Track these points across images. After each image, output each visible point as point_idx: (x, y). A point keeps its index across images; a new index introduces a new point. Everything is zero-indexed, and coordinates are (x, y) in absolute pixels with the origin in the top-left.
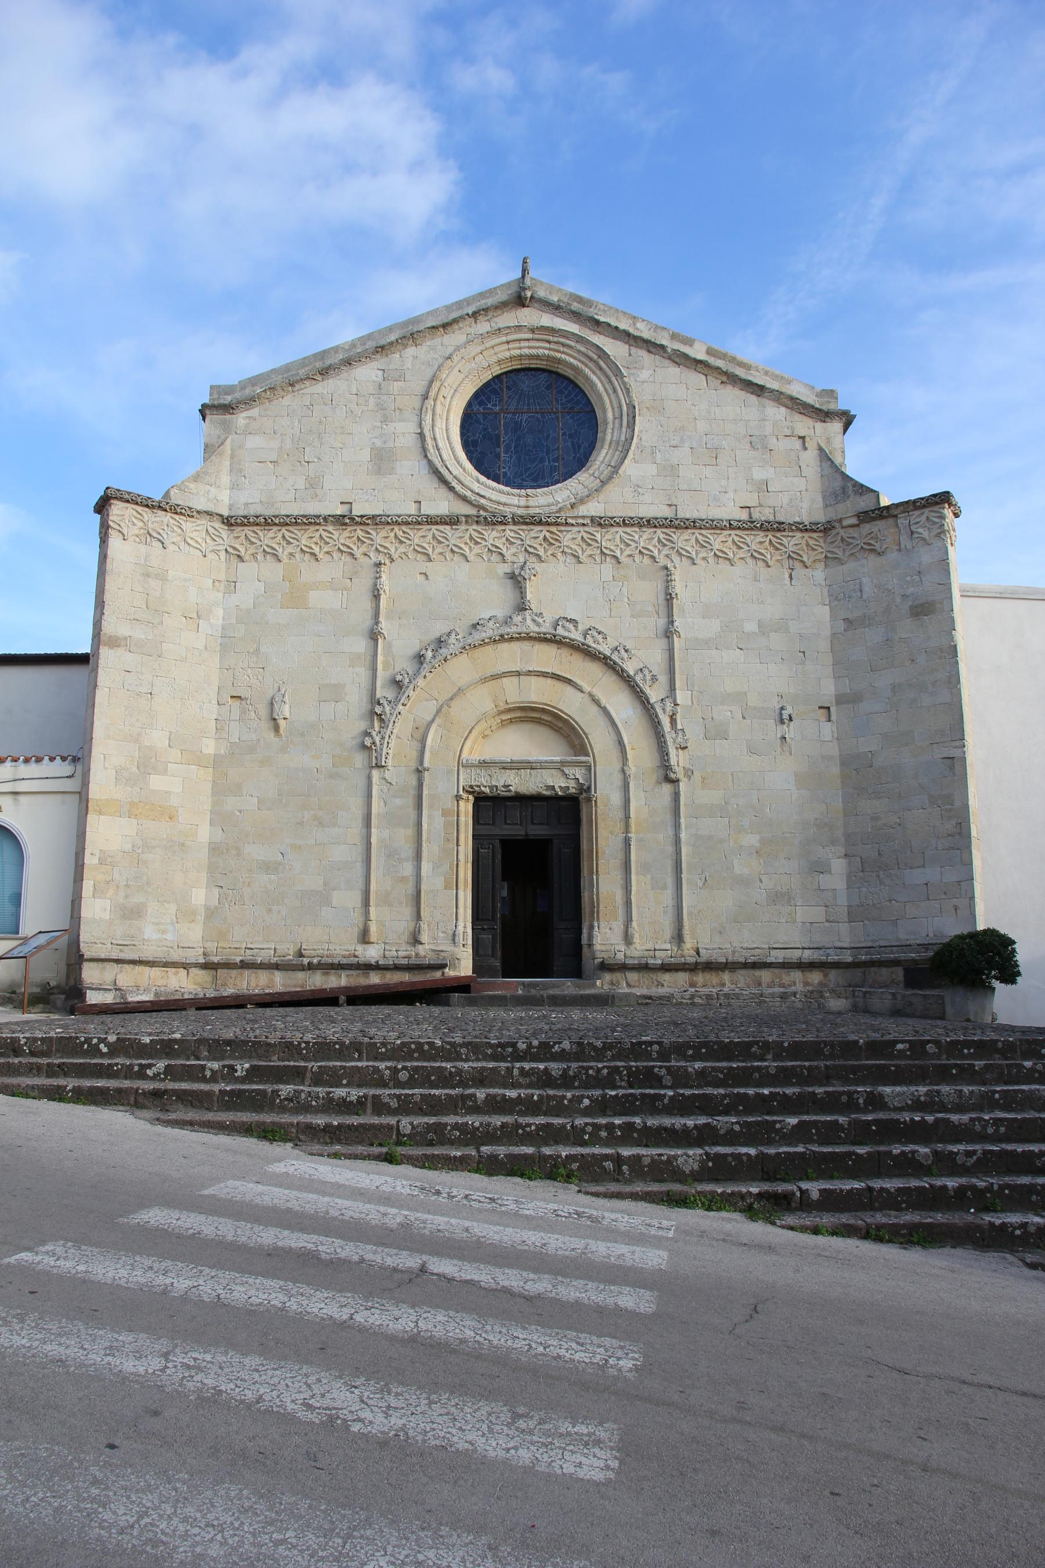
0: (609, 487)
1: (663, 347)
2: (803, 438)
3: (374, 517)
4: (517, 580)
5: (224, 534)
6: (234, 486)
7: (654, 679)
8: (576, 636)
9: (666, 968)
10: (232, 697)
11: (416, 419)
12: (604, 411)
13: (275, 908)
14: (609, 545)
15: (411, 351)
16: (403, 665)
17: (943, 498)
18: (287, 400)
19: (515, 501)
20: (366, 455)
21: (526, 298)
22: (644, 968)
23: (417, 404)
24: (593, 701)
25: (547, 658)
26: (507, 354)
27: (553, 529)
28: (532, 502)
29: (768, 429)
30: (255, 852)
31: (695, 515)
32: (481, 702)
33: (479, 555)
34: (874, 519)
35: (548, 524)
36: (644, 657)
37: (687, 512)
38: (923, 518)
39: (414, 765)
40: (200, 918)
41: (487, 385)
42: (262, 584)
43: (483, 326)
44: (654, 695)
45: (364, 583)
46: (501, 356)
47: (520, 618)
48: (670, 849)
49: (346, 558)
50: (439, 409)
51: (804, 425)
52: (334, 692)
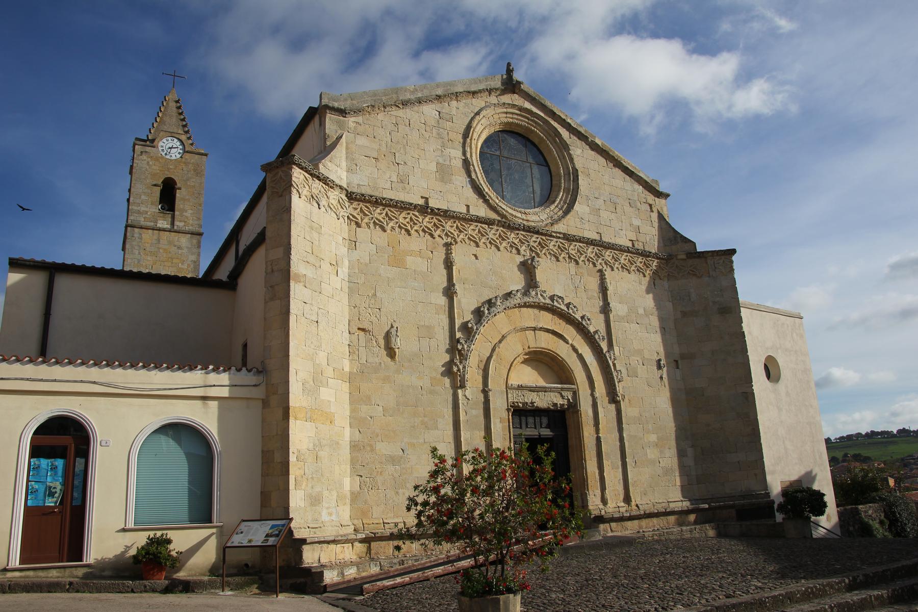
0: (568, 217)
2: (650, 205)
3: (446, 211)
4: (528, 269)
5: (347, 204)
6: (349, 170)
7: (603, 339)
8: (564, 307)
9: (631, 518)
10: (359, 329)
12: (559, 168)
13: (401, 491)
14: (573, 252)
15: (454, 103)
16: (469, 317)
17: (733, 251)
18: (381, 116)
20: (433, 167)
22: (621, 519)
23: (461, 141)
24: (570, 348)
25: (547, 320)
26: (506, 120)
28: (529, 218)
29: (636, 198)
30: (383, 448)
32: (514, 348)
33: (505, 248)
34: (694, 257)
35: (542, 234)
36: (596, 325)
37: (606, 239)
38: (721, 261)
39: (481, 387)
40: (348, 501)
42: (374, 246)
43: (493, 99)
44: (604, 346)
45: (441, 254)
47: (534, 293)
48: (618, 444)
49: (428, 237)
51: (651, 198)
52: (426, 331)
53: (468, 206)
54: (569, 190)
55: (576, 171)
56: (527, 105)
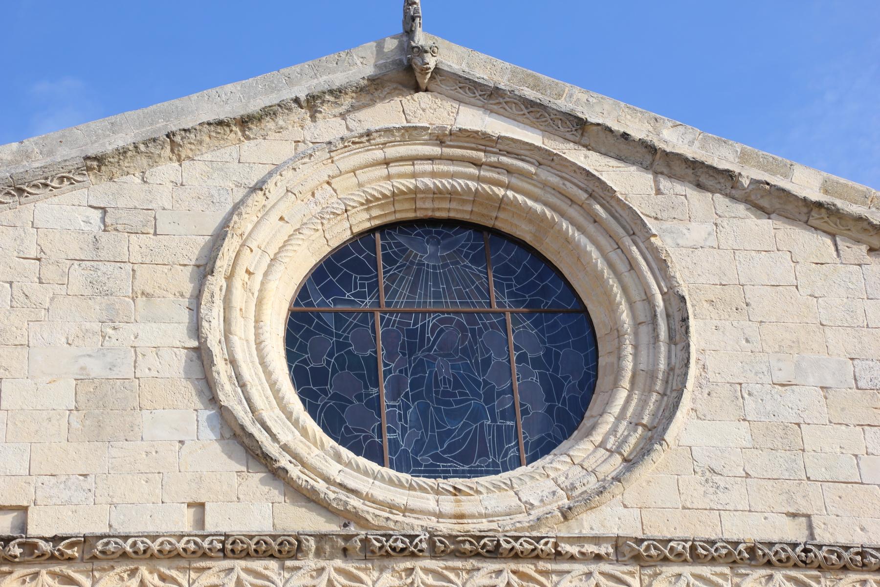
0: (645, 471)
1: (729, 175)
3: (87, 541)
11: (185, 316)
12: (612, 308)
15: (167, 171)
19: (429, 502)
20: (63, 395)
21: (424, 71)
23: (188, 288)
26: (387, 188)
27: (528, 568)
28: (468, 505)
31: (858, 539)
35: (516, 556)
37: (835, 531)
41: (340, 253)
43: (330, 126)
46: (373, 189)
50: (239, 297)
53: (200, 506)
54: (652, 375)
55: (677, 303)
56: (472, 119)
